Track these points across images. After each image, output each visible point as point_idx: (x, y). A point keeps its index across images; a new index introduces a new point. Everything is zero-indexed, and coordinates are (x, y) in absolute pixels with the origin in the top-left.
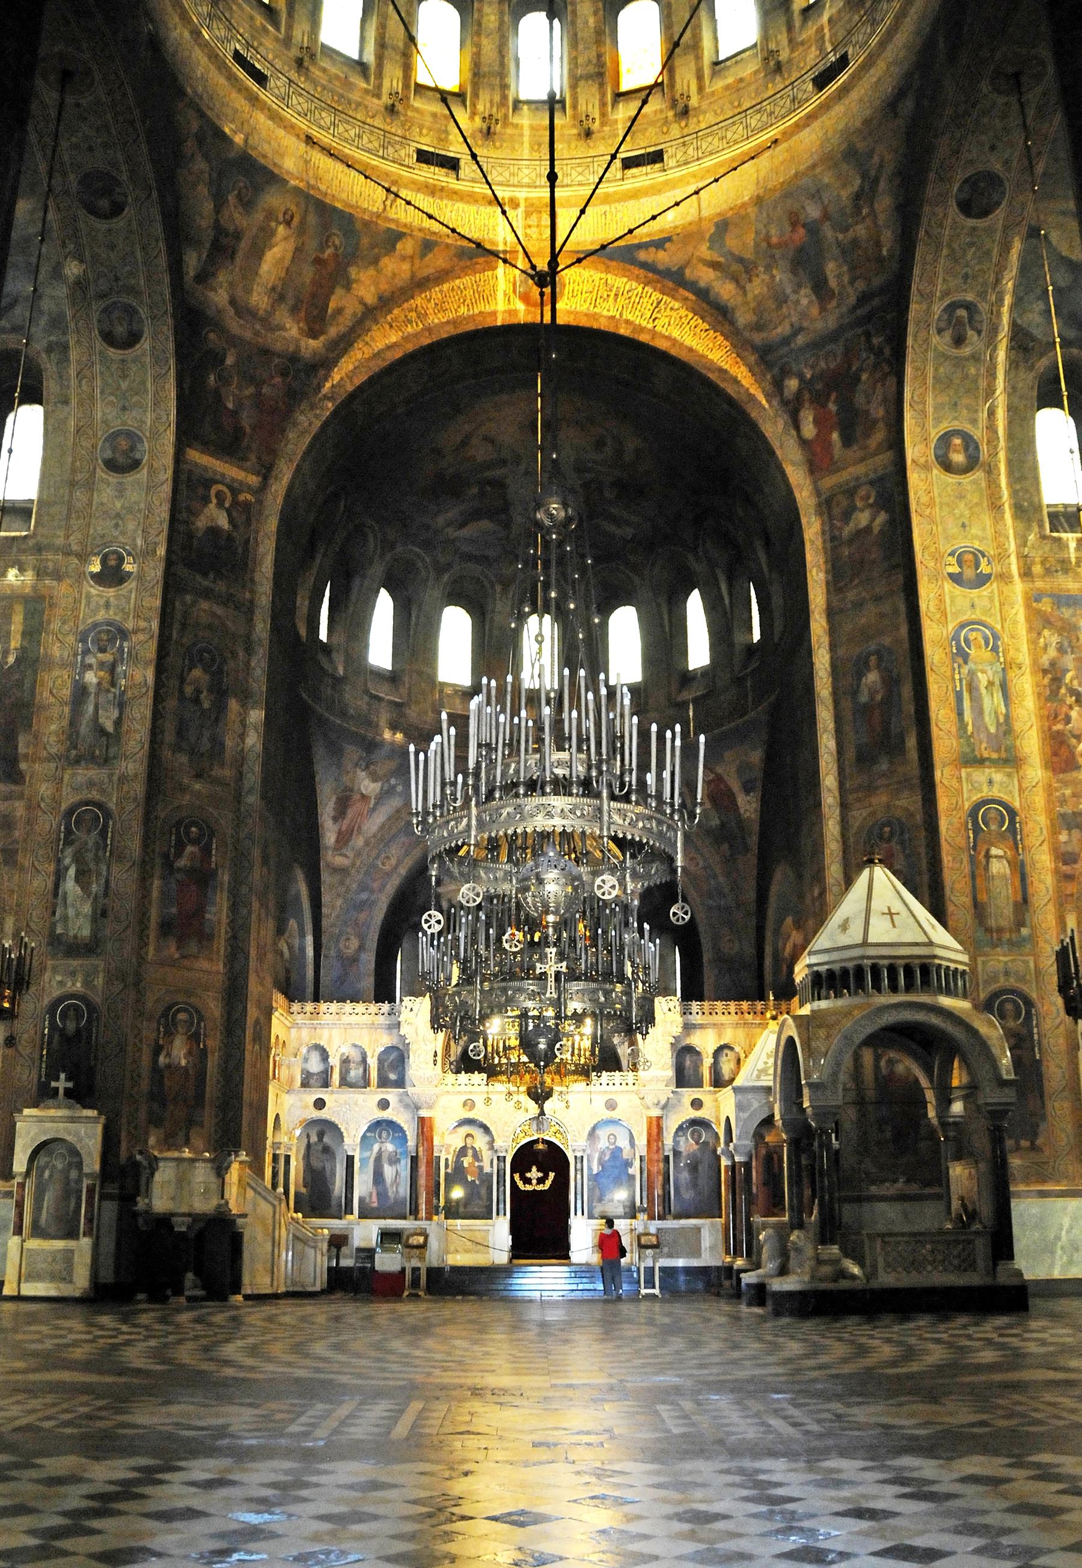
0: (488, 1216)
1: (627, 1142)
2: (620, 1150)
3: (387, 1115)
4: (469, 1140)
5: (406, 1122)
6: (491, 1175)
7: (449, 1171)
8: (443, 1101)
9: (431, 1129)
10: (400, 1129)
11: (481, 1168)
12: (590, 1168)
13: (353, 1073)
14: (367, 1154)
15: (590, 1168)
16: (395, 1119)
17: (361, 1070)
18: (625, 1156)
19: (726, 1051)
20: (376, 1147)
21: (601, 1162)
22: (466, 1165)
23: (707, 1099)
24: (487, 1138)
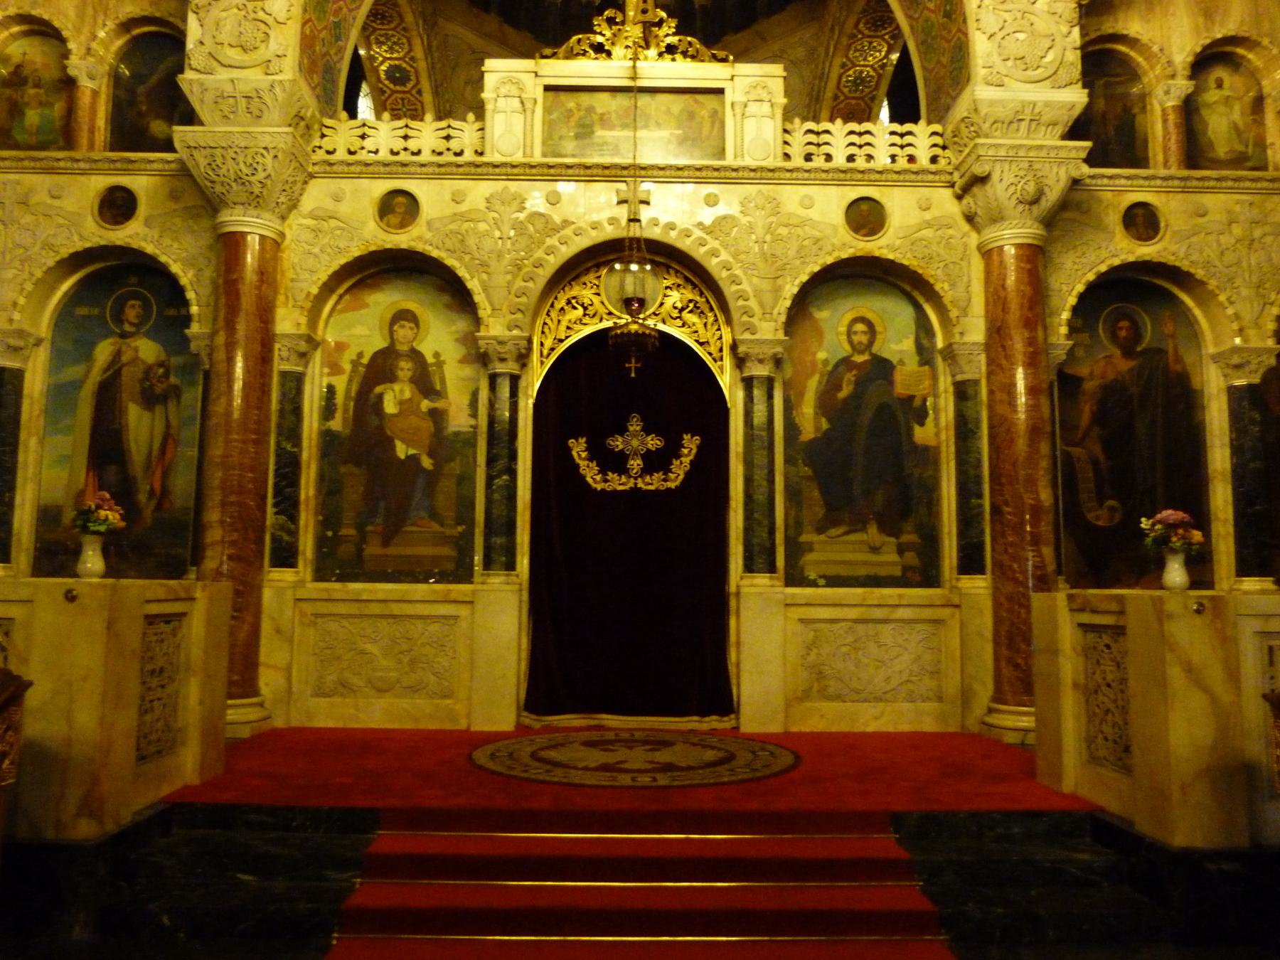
0: (462, 573)
1: (908, 345)
2: (882, 368)
3: (132, 234)
4: (404, 332)
5: (188, 263)
6: (470, 441)
7: (336, 424)
8: (316, 195)
9: (268, 275)
10: (173, 291)
11: (437, 416)
12: (792, 429)
13: (32, 117)
14: (72, 372)
15: (792, 429)
16: (150, 249)
17: (59, 108)
18: (900, 389)
19: (1220, 72)
20: (104, 351)
21: (825, 403)
22: (390, 407)
23: (1170, 206)
24: (461, 324)
